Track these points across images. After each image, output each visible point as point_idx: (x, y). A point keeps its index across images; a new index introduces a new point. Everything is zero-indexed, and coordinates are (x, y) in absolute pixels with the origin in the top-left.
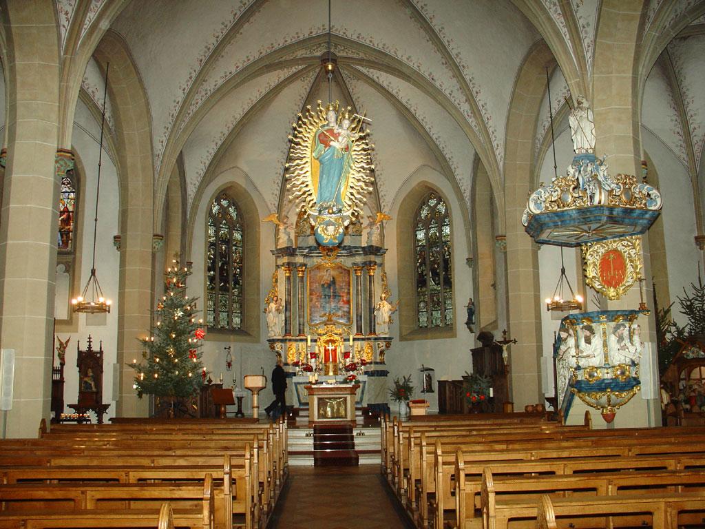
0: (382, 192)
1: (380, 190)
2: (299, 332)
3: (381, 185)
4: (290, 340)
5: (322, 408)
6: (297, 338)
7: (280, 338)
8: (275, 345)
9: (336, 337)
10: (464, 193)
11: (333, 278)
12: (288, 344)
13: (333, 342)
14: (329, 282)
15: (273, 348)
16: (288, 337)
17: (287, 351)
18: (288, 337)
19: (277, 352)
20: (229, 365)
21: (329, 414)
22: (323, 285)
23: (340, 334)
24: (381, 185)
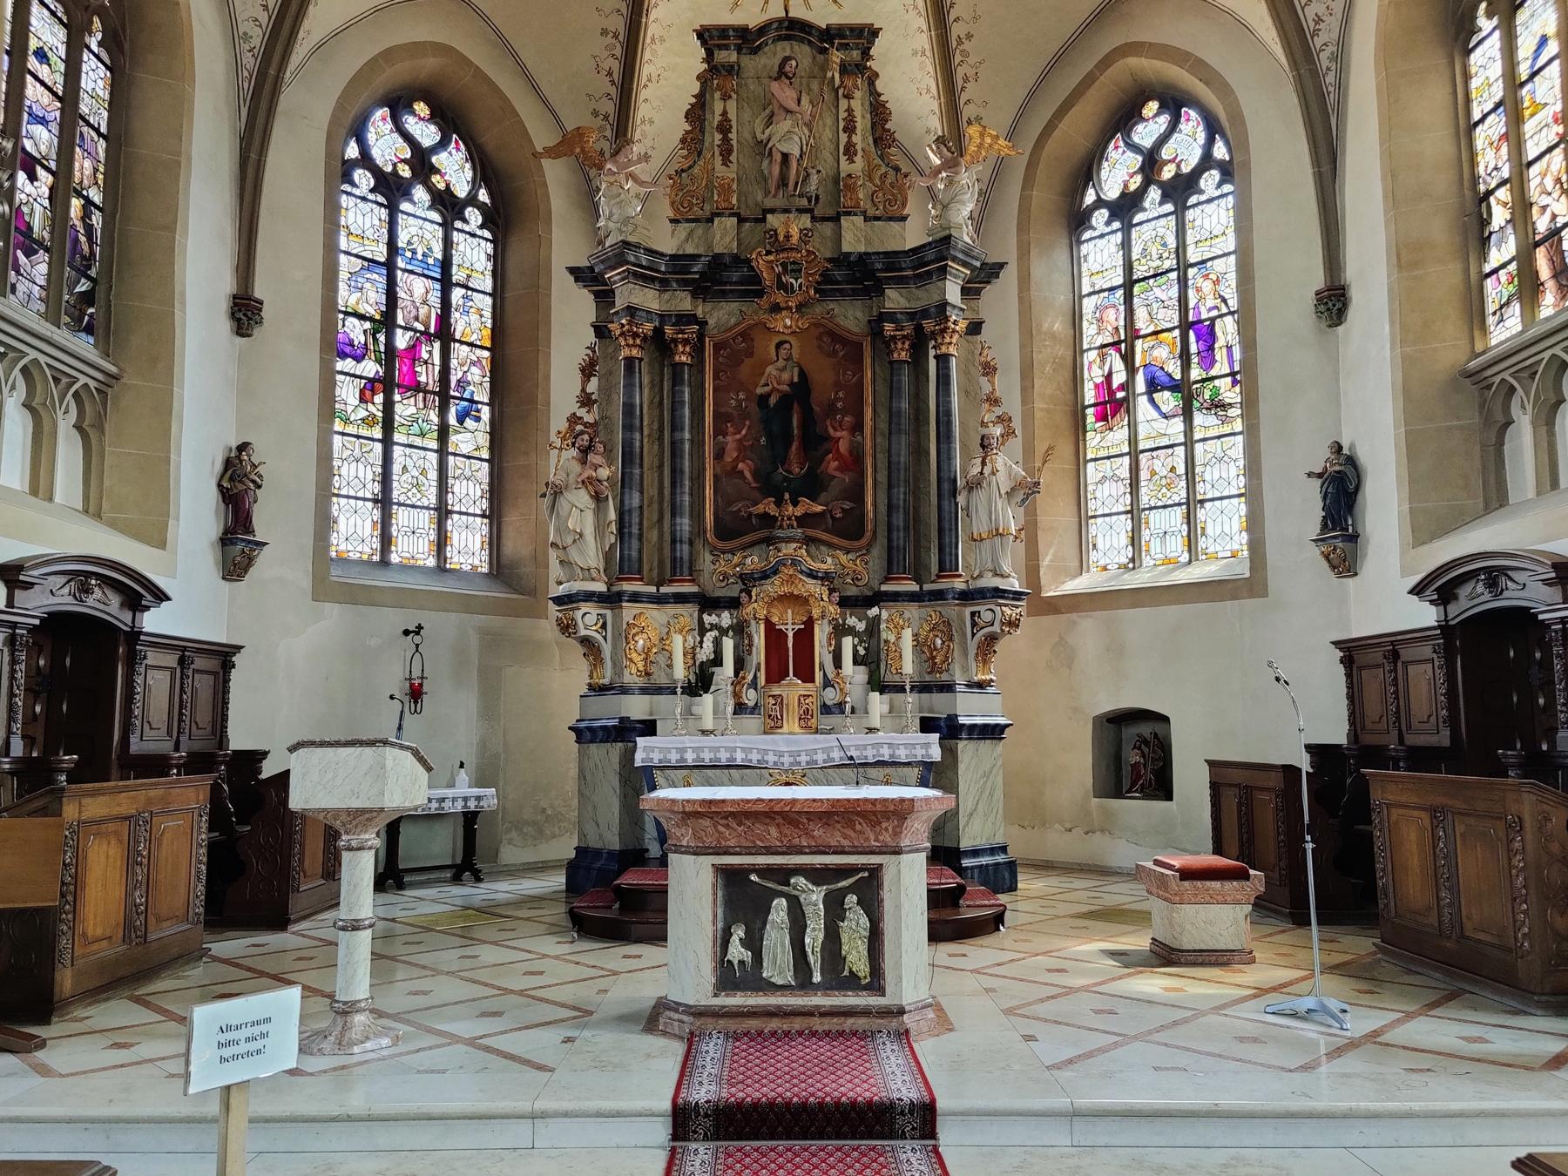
0: (971, 106)
1: (964, 97)
2: (674, 569)
3: (966, 80)
4: (635, 598)
5: (739, 932)
6: (663, 590)
7: (600, 587)
8: (579, 614)
9: (813, 587)
10: (1315, 33)
11: (802, 374)
12: (629, 611)
13: (801, 601)
14: (785, 388)
15: (567, 628)
16: (628, 587)
17: (624, 636)
18: (628, 587)
19: (586, 641)
20: (416, 694)
21: (778, 966)
22: (764, 398)
23: (826, 577)
24: (966, 80)
